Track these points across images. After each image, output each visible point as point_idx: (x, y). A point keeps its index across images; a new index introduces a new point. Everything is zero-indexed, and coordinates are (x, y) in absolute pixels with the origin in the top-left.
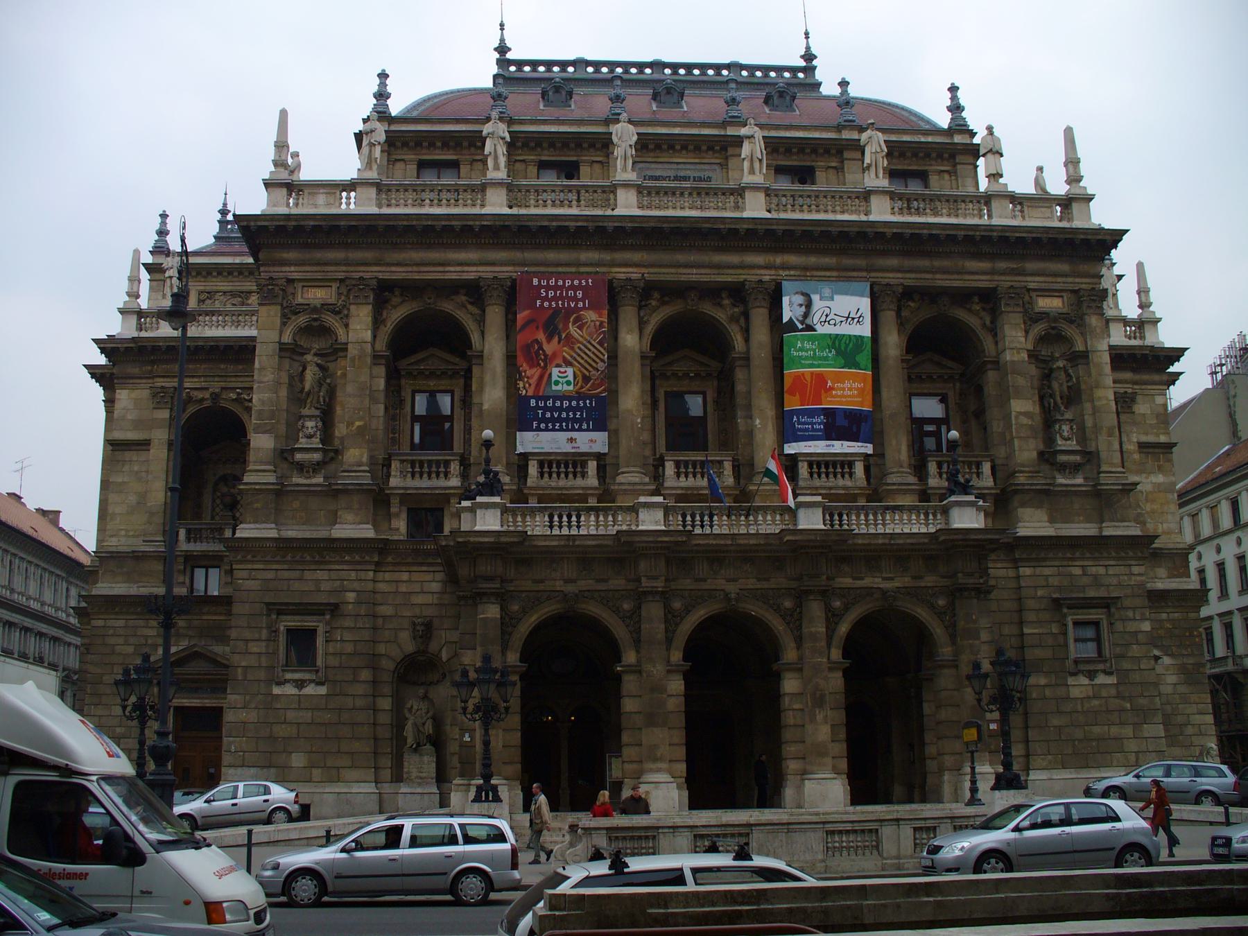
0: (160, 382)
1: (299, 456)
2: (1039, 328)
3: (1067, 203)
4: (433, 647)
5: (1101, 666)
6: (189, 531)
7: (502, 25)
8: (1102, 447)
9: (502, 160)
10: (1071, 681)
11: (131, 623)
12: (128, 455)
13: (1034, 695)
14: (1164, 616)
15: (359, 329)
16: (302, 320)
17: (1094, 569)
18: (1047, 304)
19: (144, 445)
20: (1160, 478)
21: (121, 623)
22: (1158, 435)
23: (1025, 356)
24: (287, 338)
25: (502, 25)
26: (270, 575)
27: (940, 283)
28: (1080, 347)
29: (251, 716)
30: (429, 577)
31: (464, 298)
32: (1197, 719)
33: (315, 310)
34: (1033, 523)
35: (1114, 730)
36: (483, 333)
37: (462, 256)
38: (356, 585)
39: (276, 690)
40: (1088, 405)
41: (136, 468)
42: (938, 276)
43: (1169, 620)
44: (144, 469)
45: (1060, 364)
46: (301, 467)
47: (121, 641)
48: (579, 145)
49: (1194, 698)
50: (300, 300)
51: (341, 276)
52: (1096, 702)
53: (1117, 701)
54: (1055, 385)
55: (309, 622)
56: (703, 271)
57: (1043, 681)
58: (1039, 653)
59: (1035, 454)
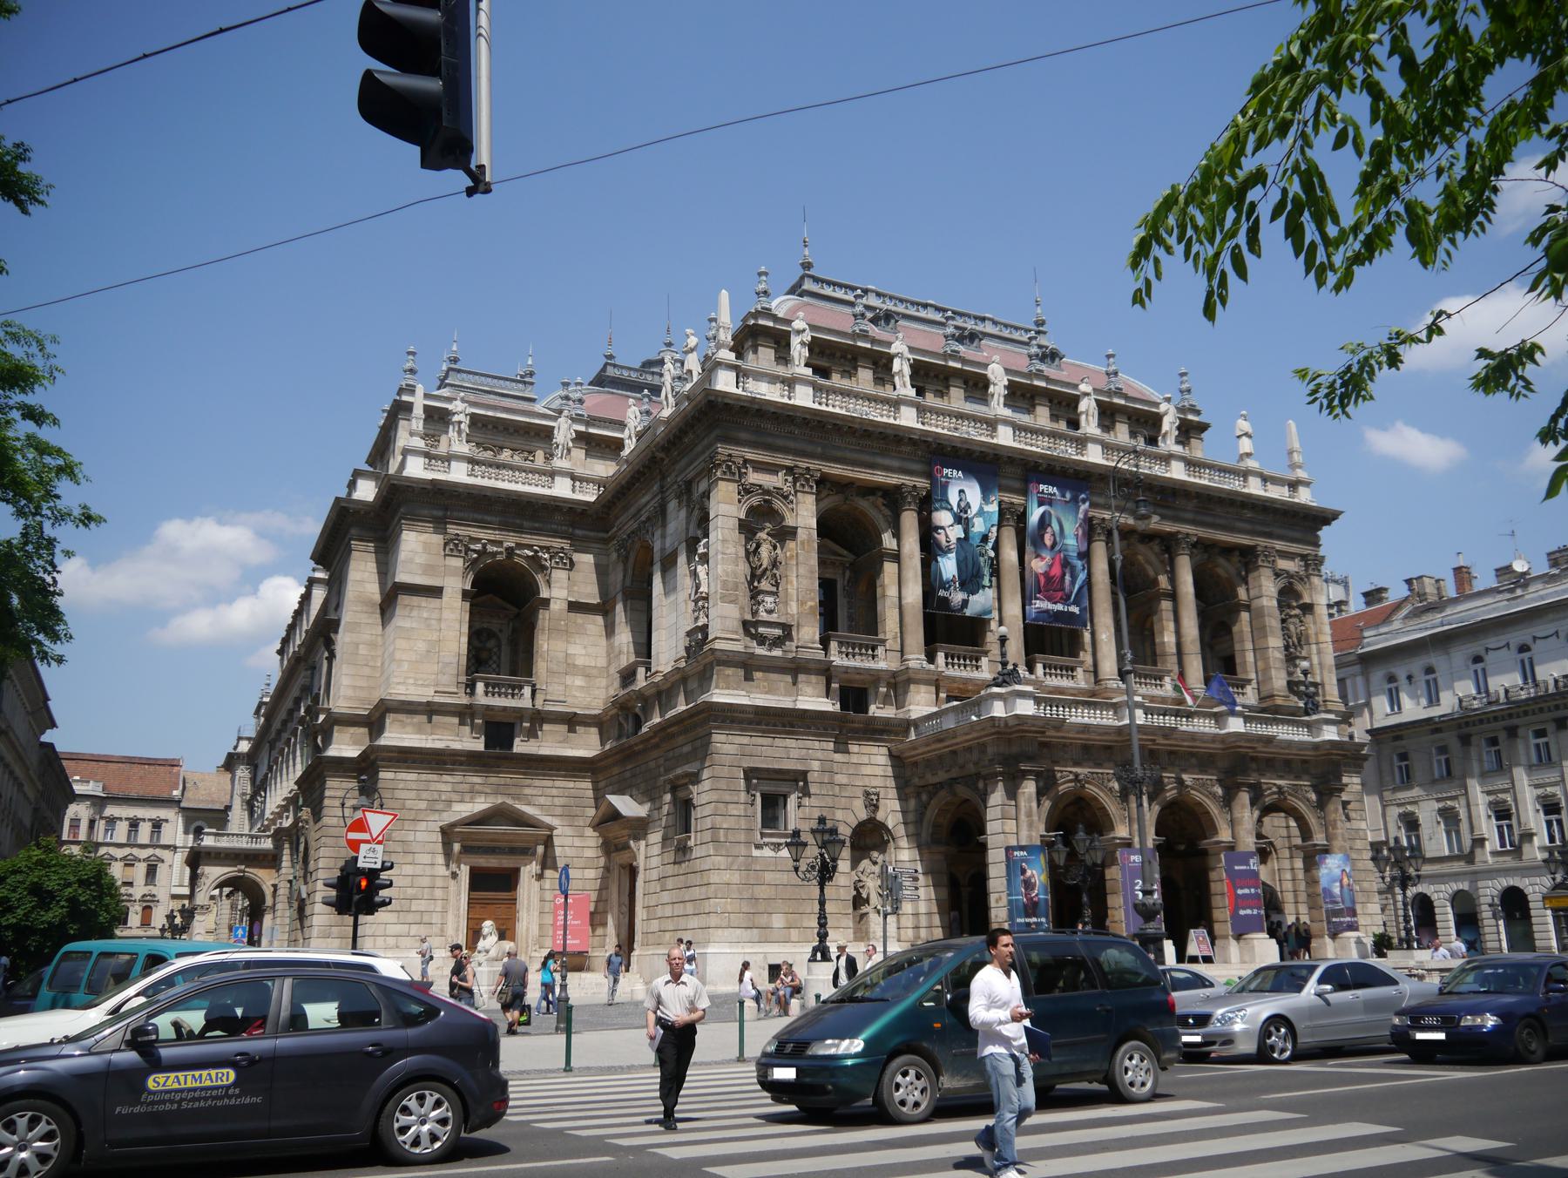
0: (452, 530)
1: (761, 630)
2: (1282, 583)
3: (1294, 485)
4: (880, 816)
6: (487, 686)
8: (1326, 680)
9: (907, 379)
11: (424, 777)
12: (415, 600)
16: (755, 500)
18: (1283, 564)
19: (435, 592)
21: (412, 776)
23: (1275, 603)
24: (742, 516)
26: (745, 740)
28: (1307, 600)
29: (735, 877)
30: (875, 750)
31: (880, 501)
33: (767, 492)
36: (897, 535)
37: (887, 462)
38: (819, 755)
39: (756, 853)
40: (1314, 647)
41: (425, 615)
44: (435, 615)
46: (761, 640)
47: (412, 794)
48: (927, 375)
50: (751, 480)
51: (788, 463)
54: (1292, 628)
55: (782, 788)
59: (1284, 683)
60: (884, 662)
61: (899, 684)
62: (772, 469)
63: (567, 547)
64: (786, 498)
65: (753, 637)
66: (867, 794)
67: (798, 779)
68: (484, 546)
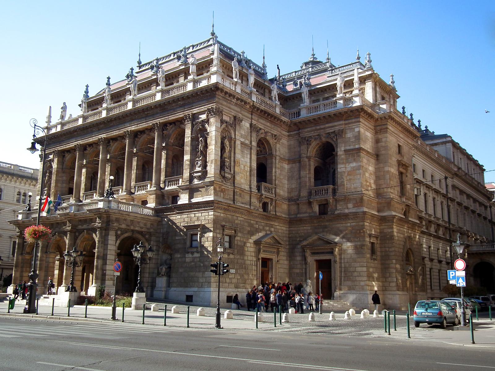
5: (195, 250)
7: (140, 55)
10: (187, 256)
13: (176, 261)
14: (349, 224)
15: (55, 165)
17: (197, 215)
20: (354, 164)
22: (355, 145)
25: (140, 55)
27: (170, 119)
32: (359, 269)
34: (184, 199)
35: (197, 274)
42: (170, 117)
43: (350, 226)
45: (200, 139)
49: (359, 260)
52: (193, 263)
53: (199, 263)
56: (116, 131)
57: (179, 256)
58: (179, 246)
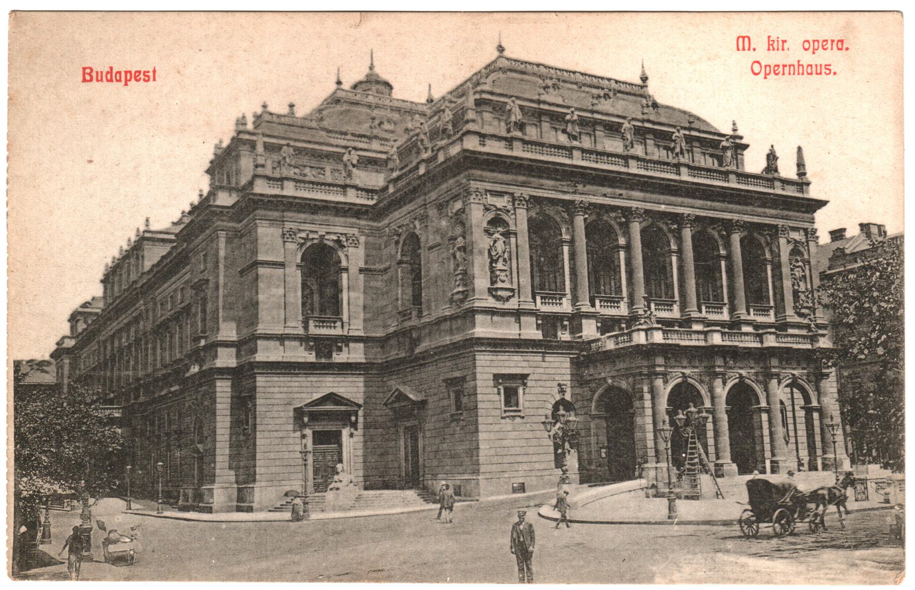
1: (499, 293)
16: (490, 216)
33: (500, 210)
46: (498, 298)
54: (797, 274)
60: (566, 307)
61: (575, 320)
62: (500, 194)
63: (356, 233)
64: (508, 211)
65: (494, 296)
66: (559, 385)
67: (523, 378)
68: (308, 235)
